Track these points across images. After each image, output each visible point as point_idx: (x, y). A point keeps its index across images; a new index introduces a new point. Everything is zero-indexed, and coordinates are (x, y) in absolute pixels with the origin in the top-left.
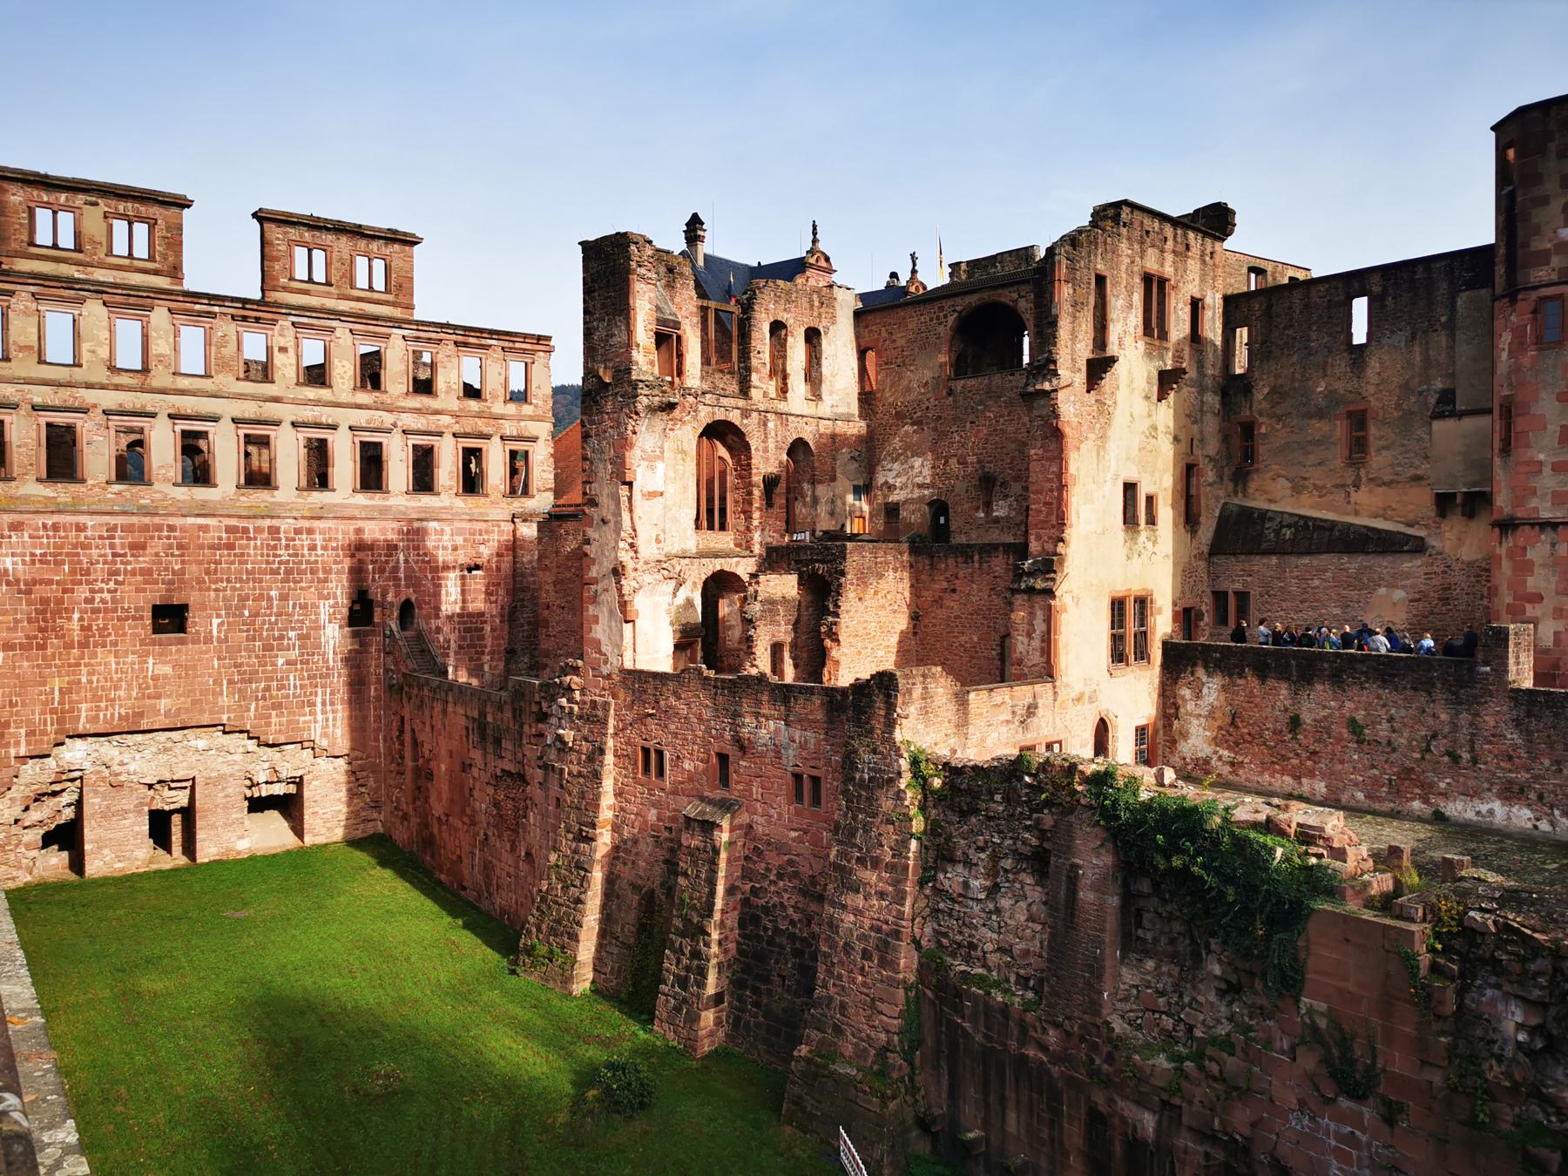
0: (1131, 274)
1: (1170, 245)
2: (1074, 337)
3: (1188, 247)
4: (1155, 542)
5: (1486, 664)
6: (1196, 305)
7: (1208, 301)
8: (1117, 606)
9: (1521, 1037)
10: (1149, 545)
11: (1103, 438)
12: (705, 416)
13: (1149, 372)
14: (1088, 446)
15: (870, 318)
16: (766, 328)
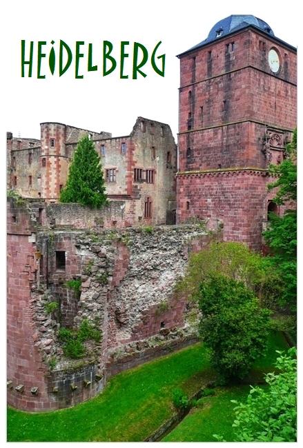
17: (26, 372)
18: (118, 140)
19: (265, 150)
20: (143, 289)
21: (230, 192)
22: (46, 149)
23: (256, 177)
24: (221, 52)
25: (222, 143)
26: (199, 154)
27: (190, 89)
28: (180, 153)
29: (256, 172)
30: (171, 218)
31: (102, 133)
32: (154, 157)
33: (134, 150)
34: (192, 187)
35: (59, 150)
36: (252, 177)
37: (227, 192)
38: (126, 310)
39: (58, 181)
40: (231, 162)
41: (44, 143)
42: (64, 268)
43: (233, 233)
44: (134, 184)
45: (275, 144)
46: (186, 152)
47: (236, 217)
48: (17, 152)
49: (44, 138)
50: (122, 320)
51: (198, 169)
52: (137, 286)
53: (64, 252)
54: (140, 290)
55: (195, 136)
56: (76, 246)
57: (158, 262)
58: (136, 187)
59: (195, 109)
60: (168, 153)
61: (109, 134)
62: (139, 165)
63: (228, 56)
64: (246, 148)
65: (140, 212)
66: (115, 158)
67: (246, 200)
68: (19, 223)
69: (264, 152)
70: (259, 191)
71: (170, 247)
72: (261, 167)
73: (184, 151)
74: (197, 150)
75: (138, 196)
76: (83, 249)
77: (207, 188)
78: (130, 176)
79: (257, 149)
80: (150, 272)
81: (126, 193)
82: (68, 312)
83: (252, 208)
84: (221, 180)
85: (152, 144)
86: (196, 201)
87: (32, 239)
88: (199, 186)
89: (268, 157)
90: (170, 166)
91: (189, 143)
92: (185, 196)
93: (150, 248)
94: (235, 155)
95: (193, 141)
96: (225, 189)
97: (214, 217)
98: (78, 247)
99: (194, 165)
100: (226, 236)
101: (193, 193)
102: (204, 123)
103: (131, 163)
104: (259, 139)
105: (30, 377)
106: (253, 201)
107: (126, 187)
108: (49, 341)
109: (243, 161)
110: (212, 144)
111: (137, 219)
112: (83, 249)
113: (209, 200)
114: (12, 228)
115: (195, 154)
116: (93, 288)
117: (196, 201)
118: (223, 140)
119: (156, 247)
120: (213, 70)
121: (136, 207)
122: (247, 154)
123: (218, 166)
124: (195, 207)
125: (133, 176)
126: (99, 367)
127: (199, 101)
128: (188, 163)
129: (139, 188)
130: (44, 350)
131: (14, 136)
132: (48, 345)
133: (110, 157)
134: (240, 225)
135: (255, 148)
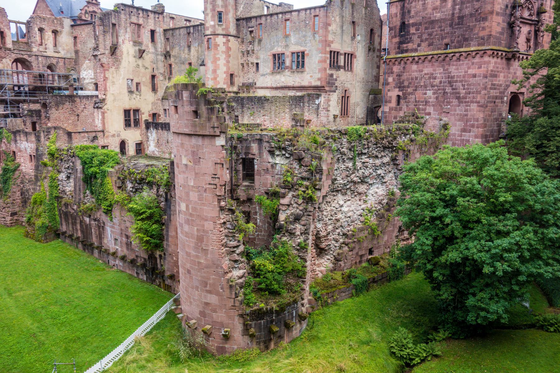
0: (126, 23)
1: (141, 15)
2: (105, 41)
3: (148, 16)
4: (140, 96)
6: (153, 32)
7: (158, 30)
8: (127, 112)
9: (131, 189)
10: (138, 96)
11: (117, 68)
12: (14, 56)
13: (135, 50)
14: (112, 70)
15: (75, 27)
16: (36, 29)
17: (215, 311)
18: (308, 12)
19: (514, 23)
20: (348, 206)
21: (461, 81)
23: (499, 60)
25: (453, 14)
26: (417, 30)
28: (391, 29)
29: (500, 53)
30: (372, 116)
31: (280, 5)
32: (354, 36)
33: (329, 25)
34: (405, 76)
35: (227, 29)
36: (493, 60)
37: (456, 81)
38: (328, 234)
39: (228, 68)
40: (465, 40)
41: (209, 18)
42: (253, 180)
43: (461, 136)
44: (329, 72)
45: (526, 14)
46: (398, 27)
47: (466, 115)
48: (171, 32)
49: (209, 11)
50: (323, 245)
51: (416, 50)
52: (341, 202)
53: (253, 159)
54: (345, 209)
56: (269, 151)
57: (367, 173)
58: (332, 75)
60: (372, 30)
61: (290, 6)
62: (335, 47)
64: (489, 18)
65: (335, 109)
67: (483, 92)
68: (203, 119)
69: (511, 26)
70: (501, 79)
71: (383, 154)
72: (505, 47)
73: (395, 27)
74: (414, 25)
75: (334, 88)
76: (278, 155)
77: (427, 76)
78: (325, 62)
79: (504, 21)
80: (357, 186)
81: (318, 83)
82: (258, 235)
83: (491, 102)
84: (449, 65)
85: (353, 17)
86: (409, 94)
87: (221, 141)
88: (415, 74)
89: (517, 32)
90: (373, 48)
91: (403, 15)
92: (395, 87)
93: (359, 154)
94: (472, 30)
95: (409, 12)
96: (453, 77)
97: (434, 115)
98: (272, 153)
99: (410, 46)
100: (451, 141)
101: (406, 83)
103: (327, 43)
104: (507, 6)
105: (220, 316)
106: (493, 93)
107: (319, 76)
108: (241, 272)
109: (483, 38)
110: (438, 15)
111: (331, 118)
112: (278, 155)
113: (430, 93)
114: (194, 125)
115: (412, 30)
116: (295, 205)
117: (409, 94)
118: (454, 9)
119: (365, 154)
121: (331, 103)
122: (491, 27)
123: (444, 46)
124: (409, 102)
125: (328, 61)
126: (303, 305)
128: (401, 43)
129: (335, 77)
130: (237, 284)
131: (166, 11)
132: (240, 278)
133: (297, 36)
134: (473, 126)
135: (500, 19)
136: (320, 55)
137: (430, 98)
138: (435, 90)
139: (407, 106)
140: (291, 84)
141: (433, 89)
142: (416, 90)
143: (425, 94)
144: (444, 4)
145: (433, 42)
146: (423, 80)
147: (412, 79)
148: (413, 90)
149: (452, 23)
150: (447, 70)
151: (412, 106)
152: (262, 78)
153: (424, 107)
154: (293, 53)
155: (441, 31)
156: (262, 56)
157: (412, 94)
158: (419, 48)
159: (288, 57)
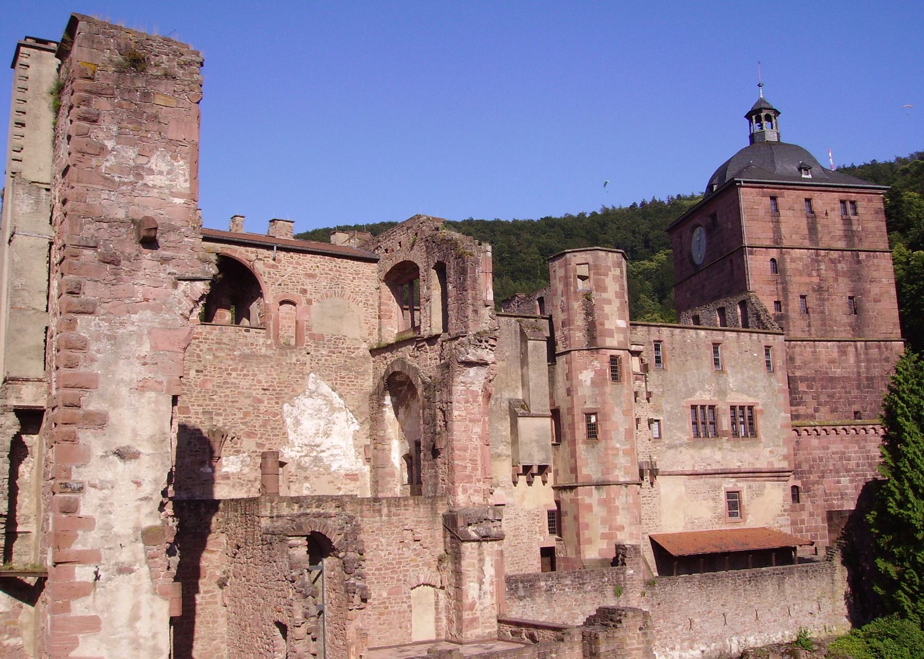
5: (632, 568)
22: (619, 329)
24: (833, 210)
25: (859, 373)
27: (774, 253)
51: (812, 417)
55: (797, 349)
59: (790, 297)
63: (848, 222)
66: (753, 379)
86: (813, 483)
101: (805, 467)
102: (813, 329)
110: (838, 372)
113: (845, 481)
117: (813, 483)
118: (859, 367)
120: (820, 236)
127: (798, 284)
133: (739, 376)
136: (783, 414)
137: (847, 488)
138: (852, 476)
139: (813, 502)
140: (734, 465)
141: (848, 476)
142: (823, 477)
143: (839, 482)
144: (844, 357)
145: (837, 408)
146: (831, 463)
147: (814, 460)
148: (819, 477)
149: (860, 384)
150: (864, 447)
151: (821, 502)
152: (671, 452)
153: (839, 503)
154: (733, 408)
155: (846, 393)
156: (668, 407)
157: (818, 483)
158: (817, 414)
159: (725, 413)
